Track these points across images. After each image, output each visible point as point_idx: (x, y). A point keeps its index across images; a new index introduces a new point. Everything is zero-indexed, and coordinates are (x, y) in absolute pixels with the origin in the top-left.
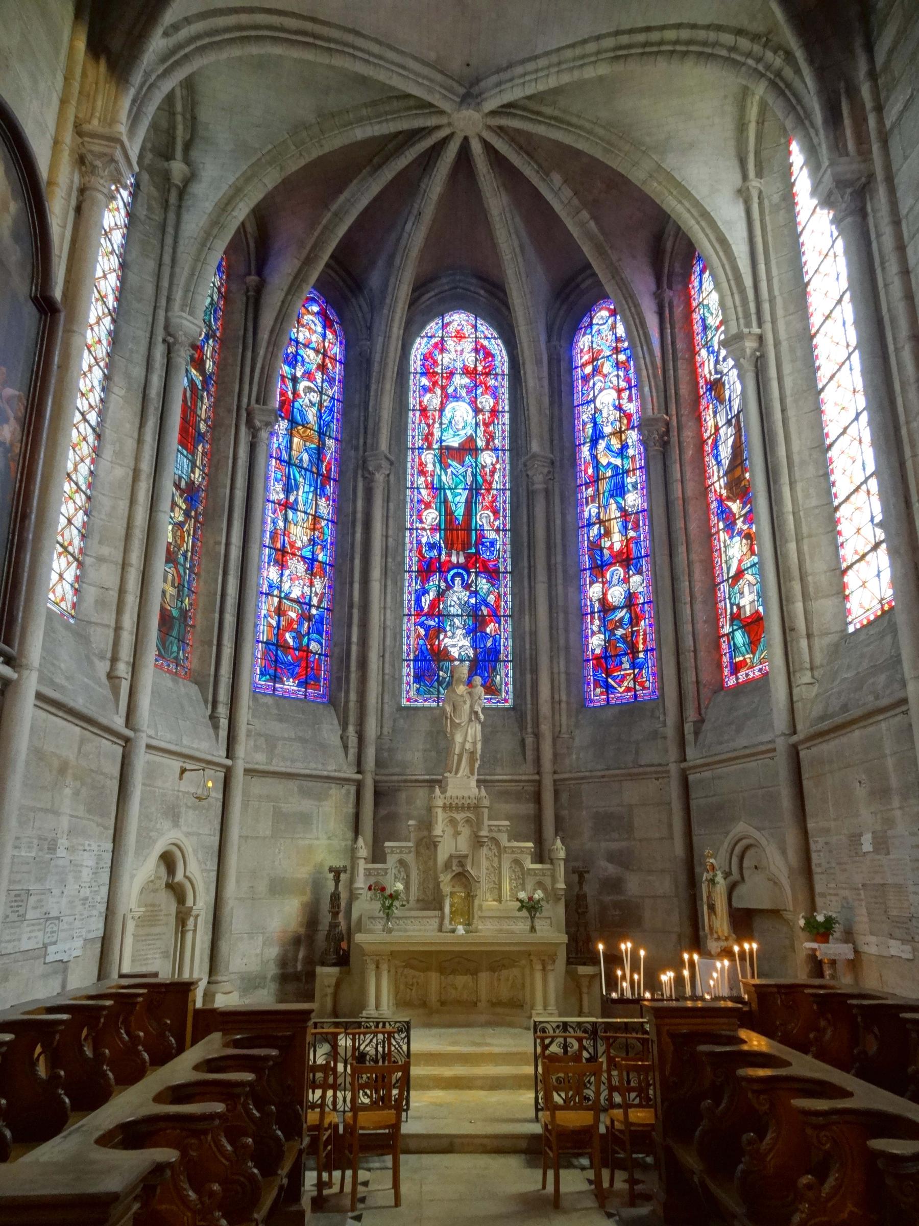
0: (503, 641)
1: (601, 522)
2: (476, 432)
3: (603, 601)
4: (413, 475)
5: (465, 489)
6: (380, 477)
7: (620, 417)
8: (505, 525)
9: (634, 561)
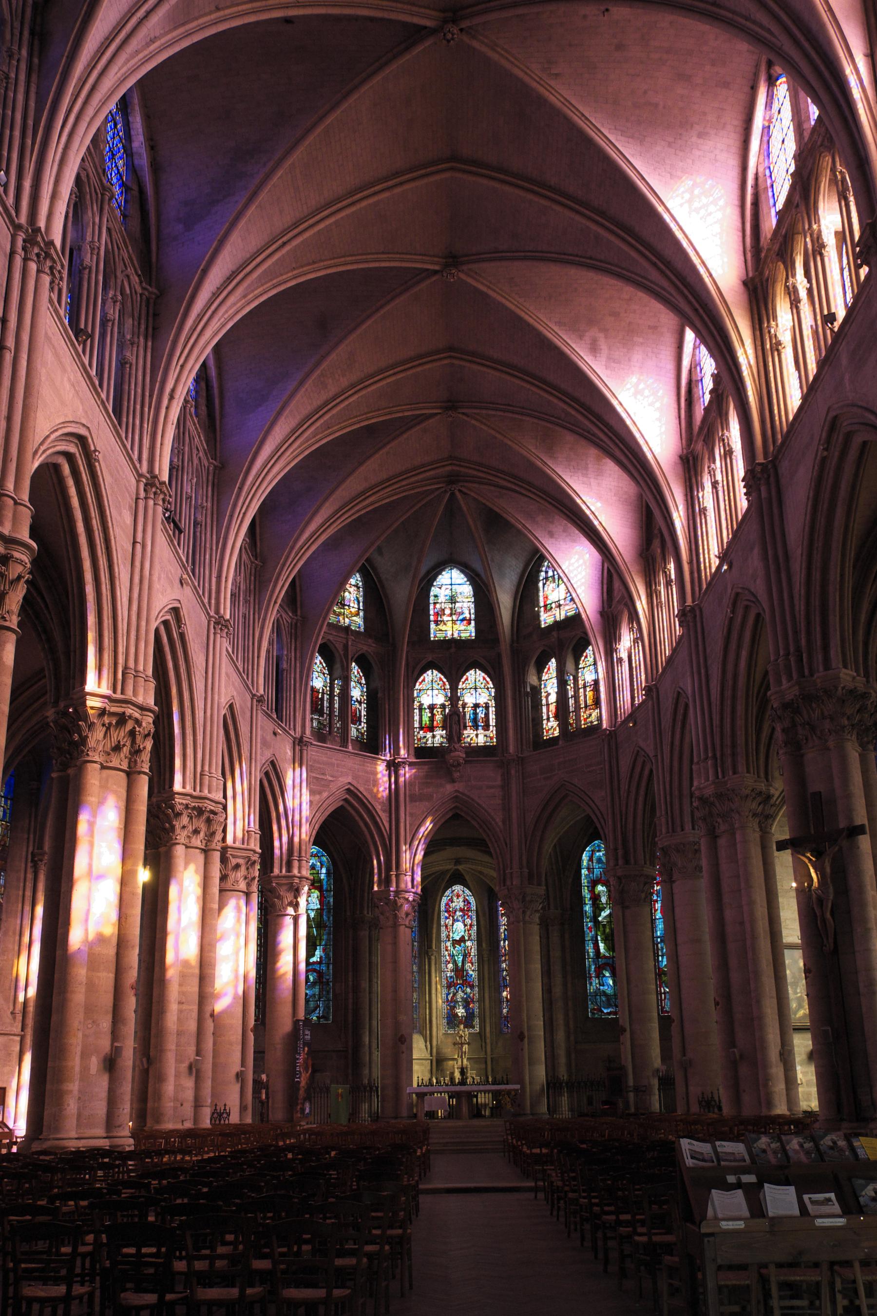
6: (433, 957)
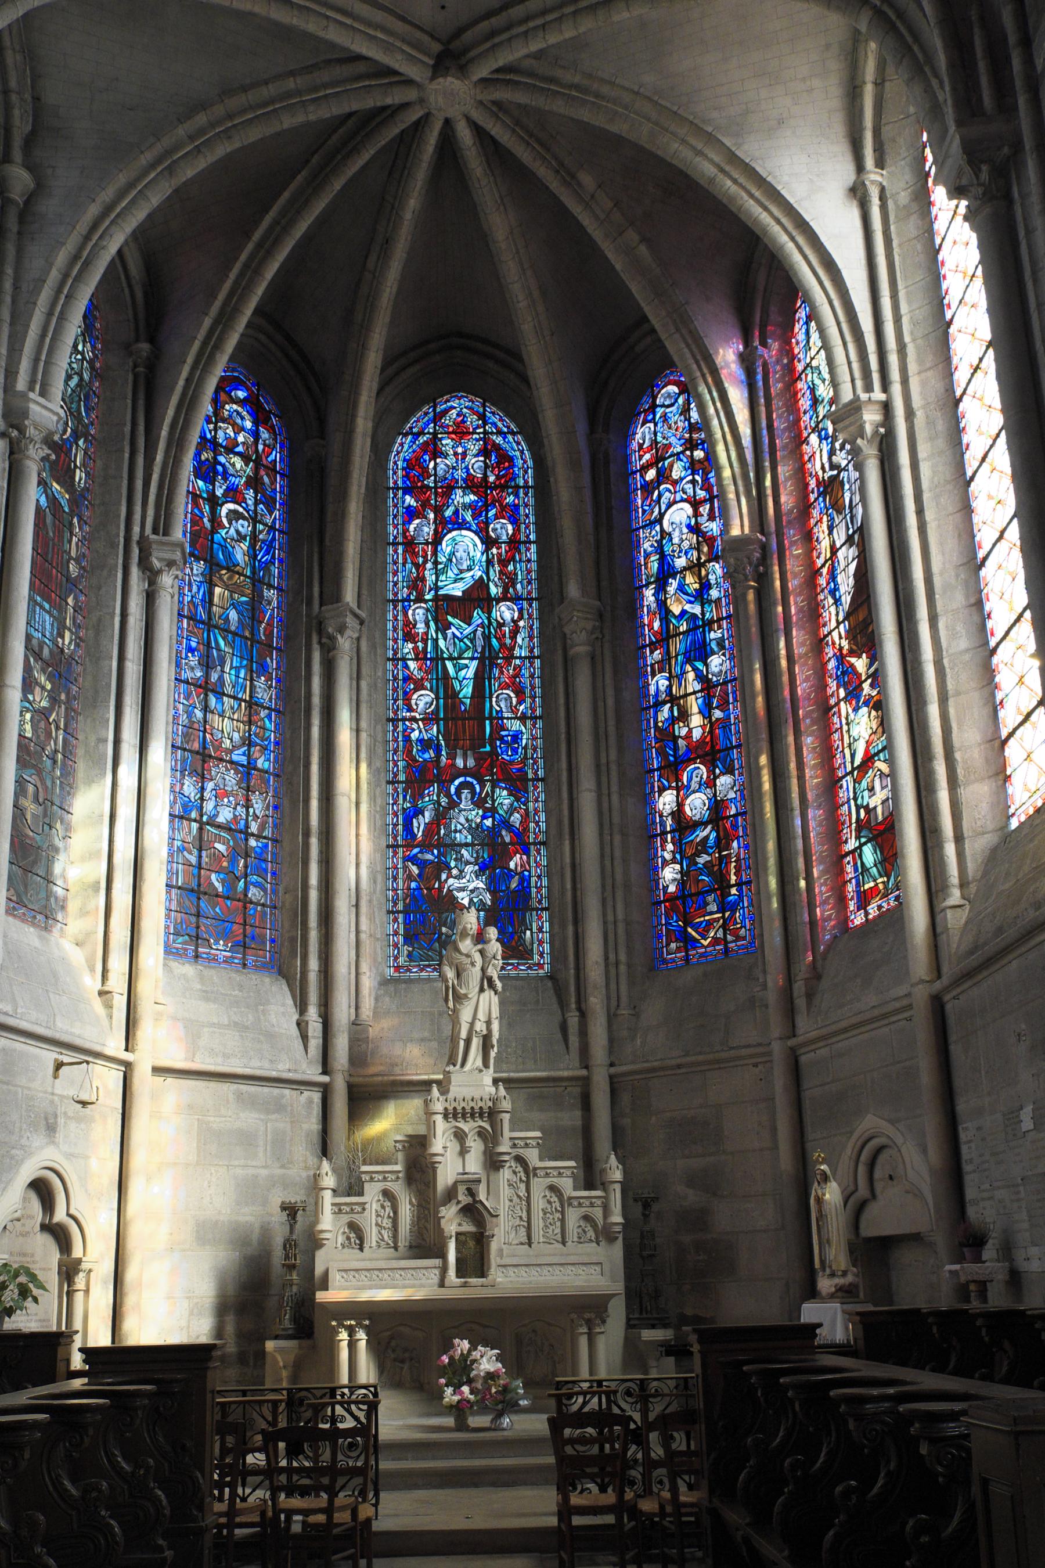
0: (533, 880)
1: (673, 699)
2: (487, 574)
3: (678, 813)
4: (395, 640)
5: (472, 659)
6: (345, 643)
7: (698, 542)
8: (534, 710)
9: (722, 754)
